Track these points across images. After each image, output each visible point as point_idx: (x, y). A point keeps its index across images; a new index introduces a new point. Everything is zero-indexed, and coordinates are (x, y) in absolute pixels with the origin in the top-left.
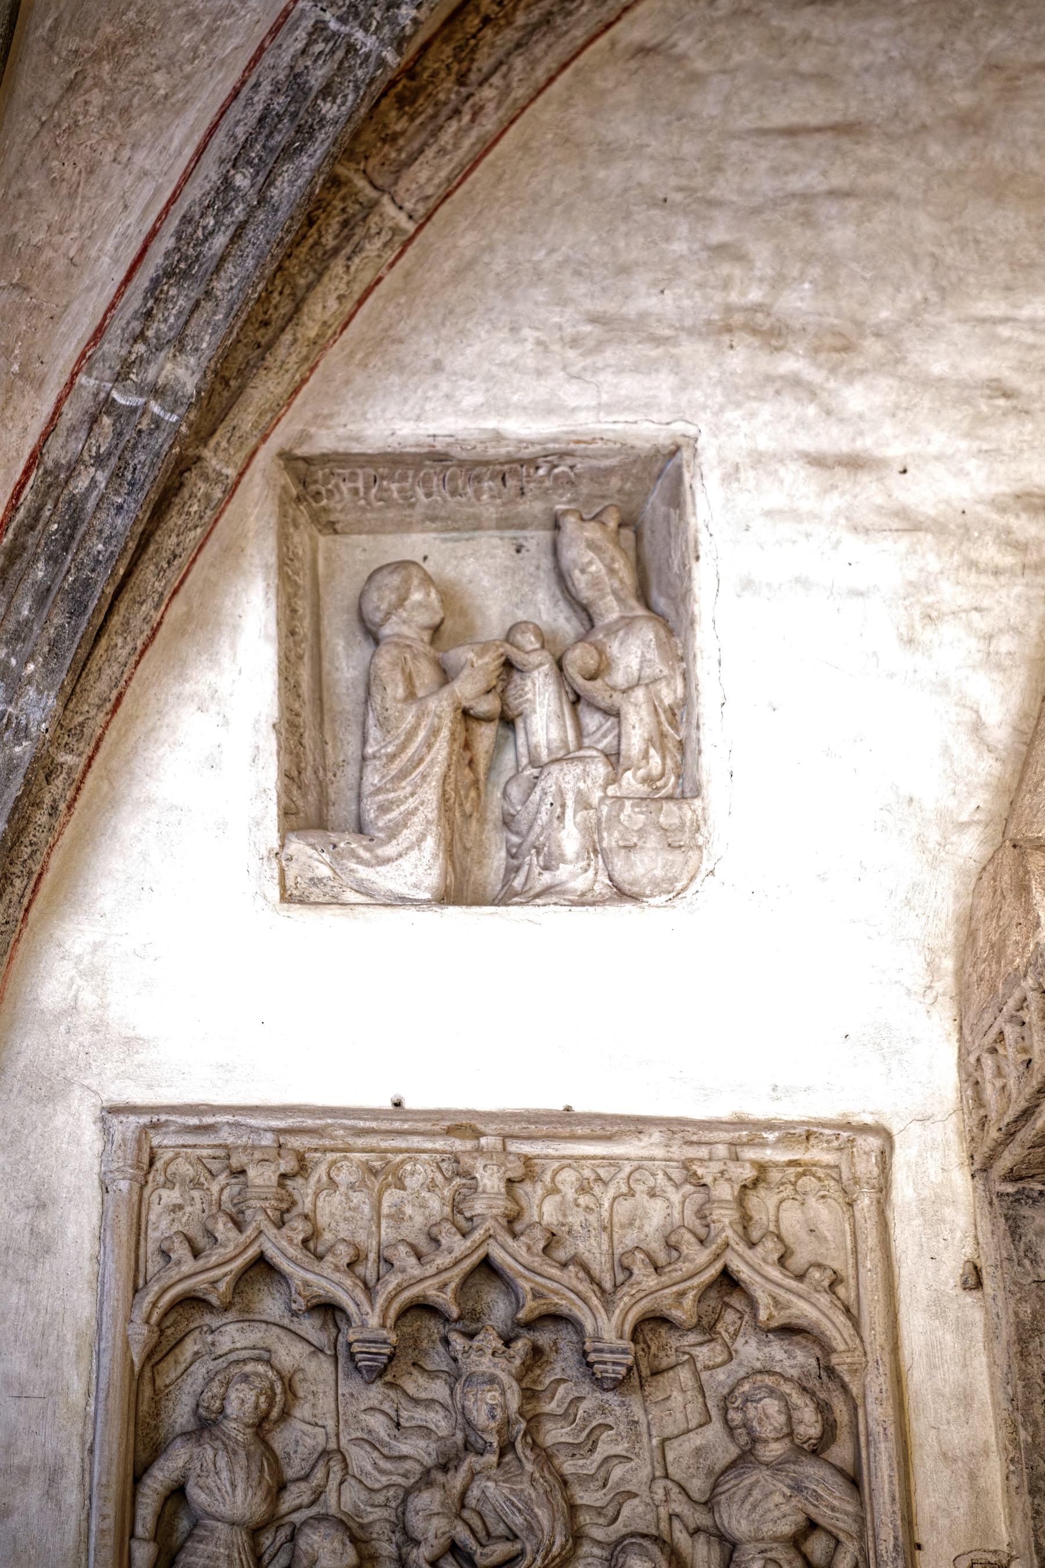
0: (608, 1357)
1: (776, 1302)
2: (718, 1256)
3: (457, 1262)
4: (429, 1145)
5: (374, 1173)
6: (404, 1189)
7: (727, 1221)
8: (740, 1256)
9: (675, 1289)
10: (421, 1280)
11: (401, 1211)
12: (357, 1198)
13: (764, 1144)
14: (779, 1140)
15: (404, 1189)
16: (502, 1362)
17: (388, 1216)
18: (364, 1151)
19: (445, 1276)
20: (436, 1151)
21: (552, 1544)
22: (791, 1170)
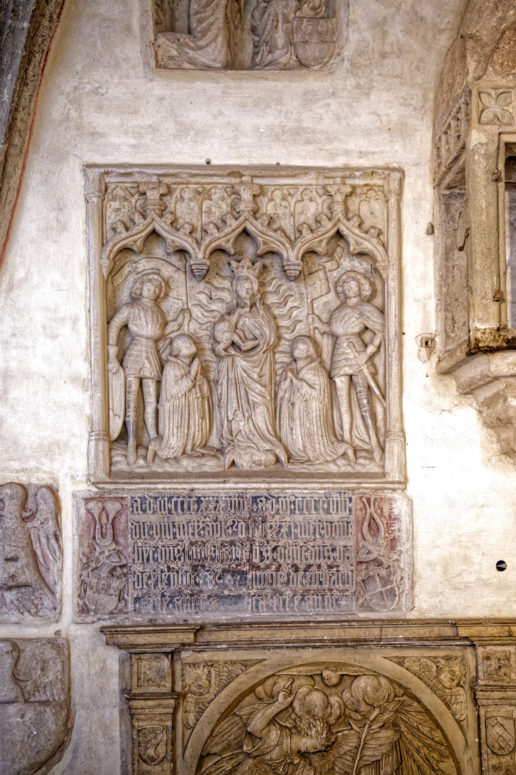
0: (292, 267)
1: (357, 243)
2: (335, 225)
3: (233, 231)
4: (221, 181)
5: (199, 193)
6: (211, 200)
7: (339, 210)
8: (344, 224)
9: (318, 239)
10: (219, 238)
11: (210, 210)
12: (193, 204)
13: (355, 177)
14: (361, 175)
15: (211, 200)
16: (251, 271)
17: (205, 212)
18: (195, 184)
19: (229, 237)
20: (224, 184)
21: (270, 341)
22: (365, 188)
